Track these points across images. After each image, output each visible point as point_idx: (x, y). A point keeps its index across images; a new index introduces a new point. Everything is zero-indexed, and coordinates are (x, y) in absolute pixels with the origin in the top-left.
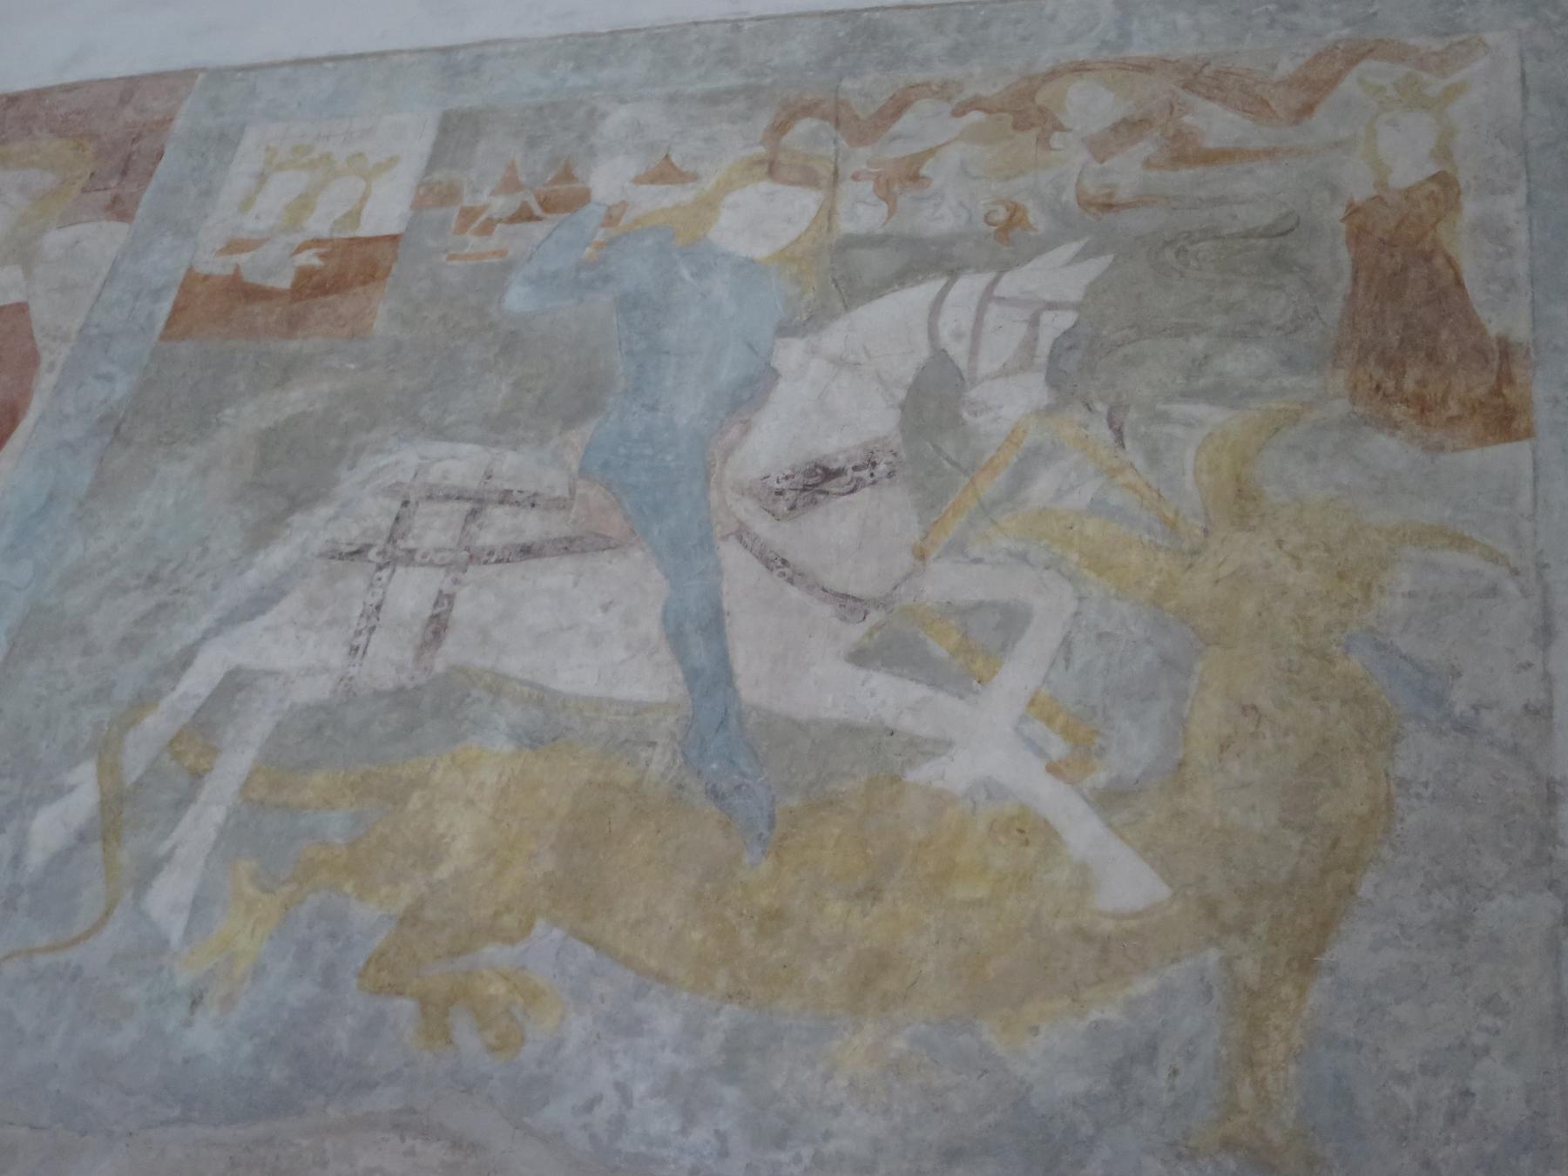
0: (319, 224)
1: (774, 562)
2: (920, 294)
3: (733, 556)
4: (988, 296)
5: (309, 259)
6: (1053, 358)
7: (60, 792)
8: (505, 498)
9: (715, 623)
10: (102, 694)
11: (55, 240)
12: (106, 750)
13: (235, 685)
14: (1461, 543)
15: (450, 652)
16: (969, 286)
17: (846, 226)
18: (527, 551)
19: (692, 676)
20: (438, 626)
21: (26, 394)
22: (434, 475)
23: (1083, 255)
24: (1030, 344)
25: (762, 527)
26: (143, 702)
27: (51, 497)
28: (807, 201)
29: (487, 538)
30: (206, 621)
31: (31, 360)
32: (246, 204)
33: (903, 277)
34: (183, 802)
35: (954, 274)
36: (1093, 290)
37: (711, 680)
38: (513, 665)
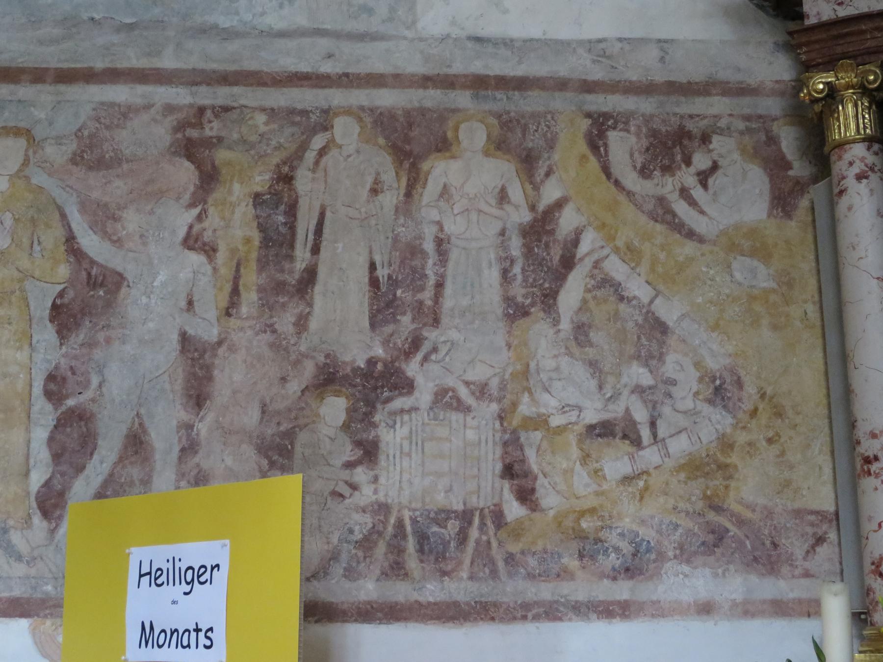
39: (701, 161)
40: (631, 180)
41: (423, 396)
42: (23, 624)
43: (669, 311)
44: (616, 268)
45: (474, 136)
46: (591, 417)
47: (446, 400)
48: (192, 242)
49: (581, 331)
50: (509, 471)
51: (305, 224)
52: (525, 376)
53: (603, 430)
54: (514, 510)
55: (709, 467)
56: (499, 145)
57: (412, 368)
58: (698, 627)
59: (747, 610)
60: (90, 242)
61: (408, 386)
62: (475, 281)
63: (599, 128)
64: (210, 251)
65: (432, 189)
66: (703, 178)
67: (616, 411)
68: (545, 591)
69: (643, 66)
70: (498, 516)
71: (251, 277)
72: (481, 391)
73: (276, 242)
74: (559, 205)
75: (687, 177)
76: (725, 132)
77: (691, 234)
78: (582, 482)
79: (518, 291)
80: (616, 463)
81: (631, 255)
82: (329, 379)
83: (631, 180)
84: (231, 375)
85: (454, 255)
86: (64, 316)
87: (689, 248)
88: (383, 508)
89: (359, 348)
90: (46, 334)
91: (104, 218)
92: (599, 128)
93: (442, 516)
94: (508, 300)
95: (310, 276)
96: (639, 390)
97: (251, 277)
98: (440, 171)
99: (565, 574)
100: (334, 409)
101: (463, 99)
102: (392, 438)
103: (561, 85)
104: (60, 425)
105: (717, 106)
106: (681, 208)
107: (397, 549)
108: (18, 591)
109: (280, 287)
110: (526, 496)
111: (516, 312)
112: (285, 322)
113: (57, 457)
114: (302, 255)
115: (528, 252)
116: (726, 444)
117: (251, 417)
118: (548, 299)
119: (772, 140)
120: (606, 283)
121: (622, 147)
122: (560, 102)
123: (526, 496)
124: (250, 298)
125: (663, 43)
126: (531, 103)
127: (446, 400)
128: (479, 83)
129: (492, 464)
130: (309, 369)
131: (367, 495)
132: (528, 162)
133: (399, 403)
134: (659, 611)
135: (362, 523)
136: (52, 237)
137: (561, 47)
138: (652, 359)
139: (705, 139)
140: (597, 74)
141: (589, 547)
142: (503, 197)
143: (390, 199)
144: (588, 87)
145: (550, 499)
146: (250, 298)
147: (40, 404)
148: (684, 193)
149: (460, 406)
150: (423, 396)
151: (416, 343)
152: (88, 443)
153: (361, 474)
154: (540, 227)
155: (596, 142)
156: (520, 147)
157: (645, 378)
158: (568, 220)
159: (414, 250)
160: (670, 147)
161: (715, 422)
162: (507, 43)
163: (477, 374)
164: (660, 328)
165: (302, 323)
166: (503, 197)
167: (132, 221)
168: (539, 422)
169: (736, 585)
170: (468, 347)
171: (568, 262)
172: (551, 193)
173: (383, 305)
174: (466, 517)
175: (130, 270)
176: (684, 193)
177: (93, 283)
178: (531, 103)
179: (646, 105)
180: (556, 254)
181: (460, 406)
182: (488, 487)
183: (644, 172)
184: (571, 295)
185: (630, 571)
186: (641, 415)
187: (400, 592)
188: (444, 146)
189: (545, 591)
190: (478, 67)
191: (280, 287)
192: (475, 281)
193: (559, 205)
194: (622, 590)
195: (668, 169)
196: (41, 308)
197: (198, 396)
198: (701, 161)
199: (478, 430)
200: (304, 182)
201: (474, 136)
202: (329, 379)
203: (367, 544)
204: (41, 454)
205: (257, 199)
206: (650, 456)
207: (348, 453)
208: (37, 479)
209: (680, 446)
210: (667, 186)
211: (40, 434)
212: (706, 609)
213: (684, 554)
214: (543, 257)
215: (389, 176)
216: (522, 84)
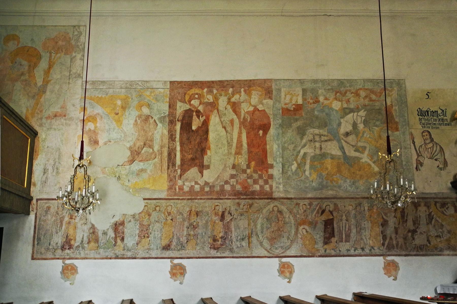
0: (294, 102)
1: (346, 142)
2: (352, 114)
3: (342, 141)
4: (357, 115)
5: (294, 106)
6: (364, 122)
7: (293, 164)
8: (322, 135)
9: (343, 148)
10: (293, 155)
11: (265, 101)
12: (296, 160)
13: (305, 154)
14: (395, 141)
15: (323, 151)
16: (356, 114)
17: (344, 107)
18: (326, 141)
19: (343, 153)
20: (321, 148)
21: (270, 121)
22: (315, 132)
23: (364, 111)
24: (361, 121)
25: (344, 138)
26: (297, 156)
27: (278, 134)
28: (340, 103)
29: (322, 139)
30: (300, 148)
31: (269, 117)
32: (285, 99)
33: (350, 113)
34: (305, 165)
35: (354, 113)
36: (366, 115)
37: (344, 153)
38: (328, 152)
39: (447, 207)
40: (439, 209)
41: (419, 233)
42: (382, 257)
43: (444, 223)
44: (438, 219)
45: (422, 204)
46: (436, 235)
47: (421, 233)
48: (395, 217)
49: (434, 226)
50: (428, 241)
51: (406, 215)
52: (429, 231)
53: (437, 236)
54: (428, 245)
55: (448, 240)
56: (425, 205)
57: (417, 230)
58: (448, 257)
59: (453, 255)
60: (384, 217)
61: (417, 232)
62: (423, 221)
63: (436, 203)
64: (396, 218)
65: (419, 210)
66: (447, 208)
67: (438, 234)
68: (432, 253)
69: (440, 196)
70: (427, 245)
71: (401, 220)
72: (425, 232)
73: (403, 216)
74: (432, 212)
75: (445, 208)
76: (450, 203)
77: (446, 215)
78: (435, 242)
79: (428, 221)
80: (439, 240)
81: (439, 217)
82: (409, 231)
83: (439, 209)
84: (400, 231)
85: (421, 218)
86: (383, 225)
87: (445, 217)
88: (415, 245)
89: (412, 228)
90: (381, 227)
91: (386, 214)
92: (436, 203)
93: (421, 245)
94: (427, 223)
95: (407, 220)
96: (441, 232)
97: (401, 220)
98: (419, 208)
99: (434, 251)
100: (410, 234)
101: (421, 200)
102: (416, 237)
103: (431, 198)
104: (383, 236)
105: (448, 200)
106: (445, 212)
107: (417, 249)
108: (382, 254)
109: (404, 221)
110: (430, 243)
111: (428, 224)
112: (405, 225)
113: (383, 240)
114: (406, 218)
115: (429, 217)
116: (450, 238)
117: (402, 235)
118: (431, 222)
119: (455, 204)
120: (436, 220)
121: (438, 205)
122: (432, 200)
123: (430, 243)
124: (401, 223)
125: (443, 193)
126: (429, 200)
127: (421, 233)
128: (423, 198)
129: (426, 240)
130: (407, 230)
131: (414, 243)
132: (428, 207)
133: (416, 233)
134: (444, 255)
135: (414, 246)
136: (381, 216)
137: (431, 193)
138: (442, 229)
139: (447, 204)
140: (435, 197)
141: (436, 248)
142: (426, 211)
143: (414, 212)
144: (434, 198)
145: (432, 244)
146: (401, 223)
147: (381, 234)
148: (445, 210)
149: (422, 234)
150: (419, 233)
151: (418, 227)
152: (386, 238)
153: (413, 241)
154: (430, 214)
155: (435, 205)
156: (428, 206)
157: (441, 231)
158: (433, 213)
159: (417, 217)
160: (443, 205)
161: (449, 235)
162: (426, 193)
163: (424, 230)
164: (442, 225)
165: (406, 225)
166: (426, 211)
167: (389, 215)
168: (430, 235)
169: (451, 253)
170: (423, 228)
171: (433, 218)
172: (431, 210)
173: (414, 224)
174: (424, 245)
175: (389, 220)
176: (445, 210)
177: (385, 221)
178: (429, 200)
179: (441, 200)
180: (431, 218)
181: (422, 234)
182: (425, 242)
183: (441, 208)
184: (433, 222)
185: (440, 251)
186: (441, 235)
187: (418, 253)
188: (420, 205)
189: (432, 253)
190: (422, 196)
191: (404, 221)
192: (423, 221)
193: (432, 212)
194: (440, 253)
195: (443, 208)
196: (380, 224)
197: (397, 233)
198: (447, 207)
199: (424, 236)
200: (405, 210)
201: (422, 204)
202: (409, 231)
203: (414, 248)
204: (382, 239)
205: (401, 212)
206: (442, 239)
207: (412, 239)
208: (382, 242)
209: (445, 238)
210: (443, 209)
211: (381, 238)
212: (448, 255)
213: (446, 249)
214: (430, 217)
215: (414, 209)
216: (427, 198)
